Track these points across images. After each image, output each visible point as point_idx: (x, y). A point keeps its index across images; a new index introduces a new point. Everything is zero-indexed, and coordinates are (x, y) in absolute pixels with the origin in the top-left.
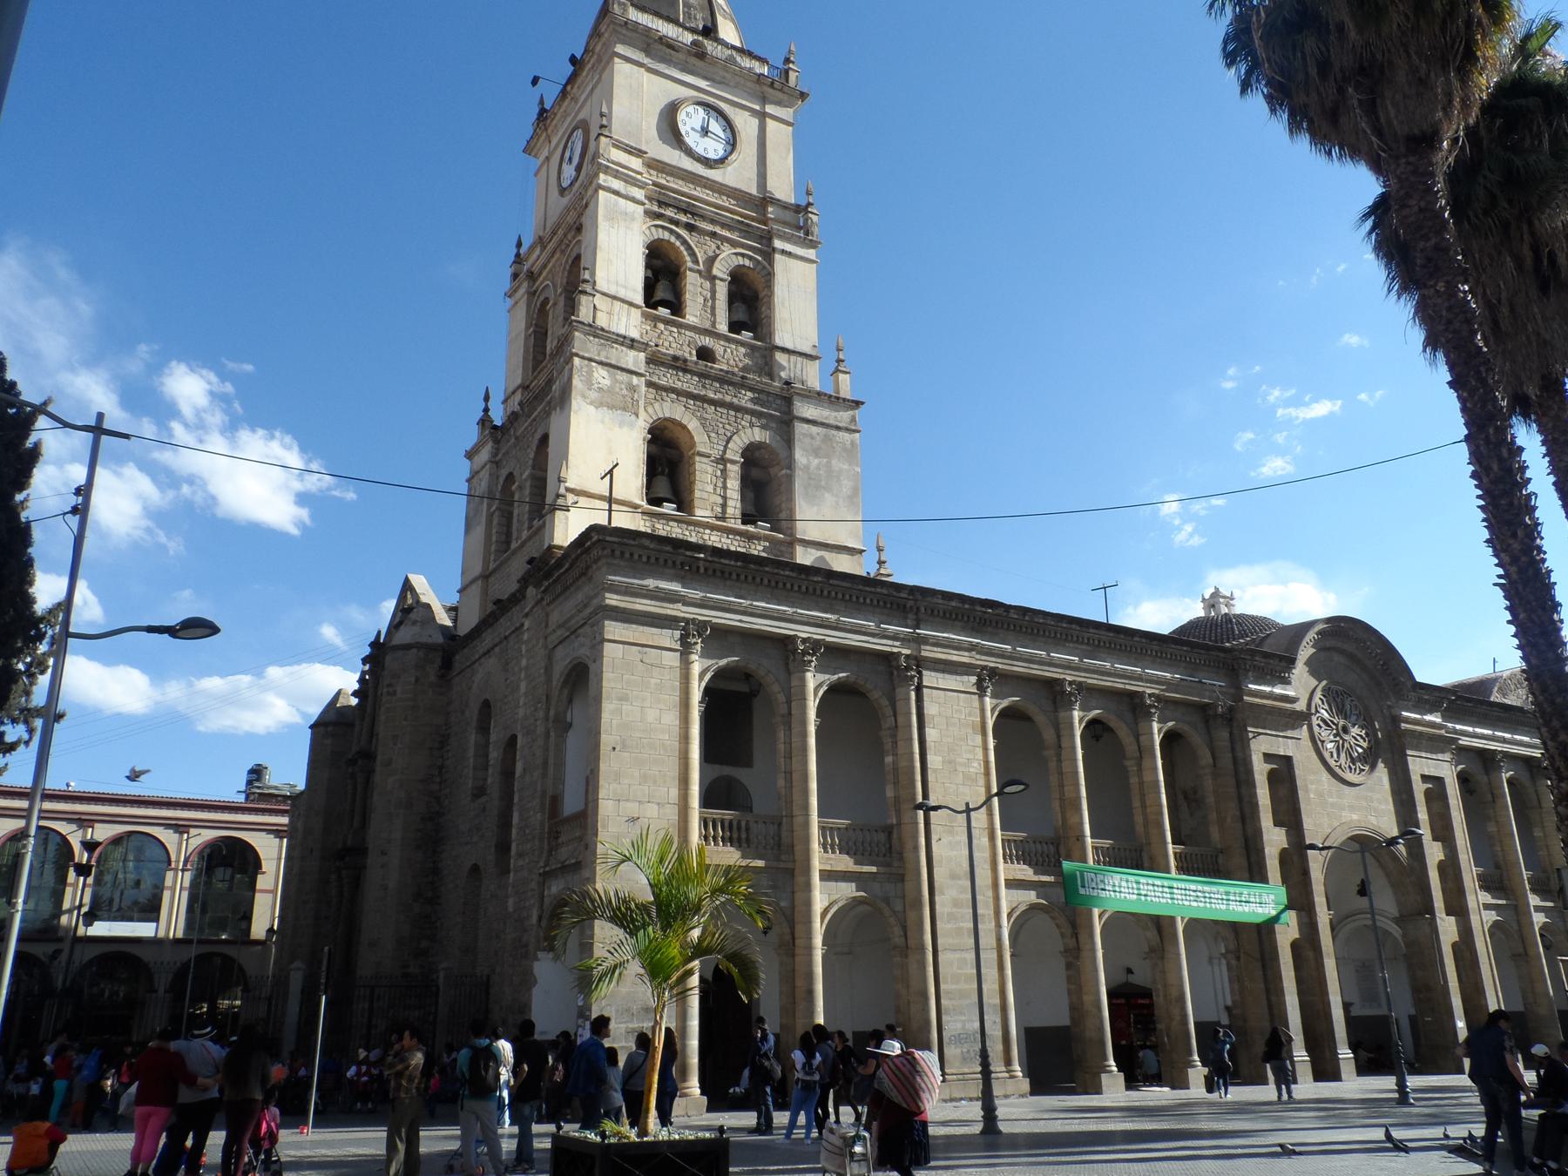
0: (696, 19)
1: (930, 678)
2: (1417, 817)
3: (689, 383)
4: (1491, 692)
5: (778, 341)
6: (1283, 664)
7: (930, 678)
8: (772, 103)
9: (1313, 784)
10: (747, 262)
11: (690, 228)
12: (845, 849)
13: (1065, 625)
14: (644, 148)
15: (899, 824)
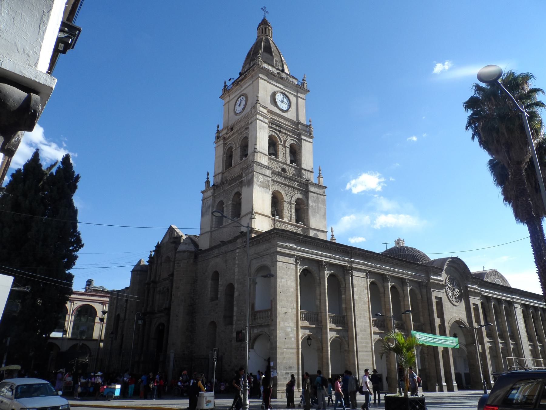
0: (278, 65)
1: (355, 273)
2: (471, 315)
3: (281, 180)
4: (484, 277)
5: (304, 166)
6: (440, 271)
7: (355, 273)
8: (299, 93)
9: (446, 304)
10: (294, 142)
11: (280, 131)
12: (334, 322)
13: (387, 258)
14: (268, 107)
15: (347, 315)
